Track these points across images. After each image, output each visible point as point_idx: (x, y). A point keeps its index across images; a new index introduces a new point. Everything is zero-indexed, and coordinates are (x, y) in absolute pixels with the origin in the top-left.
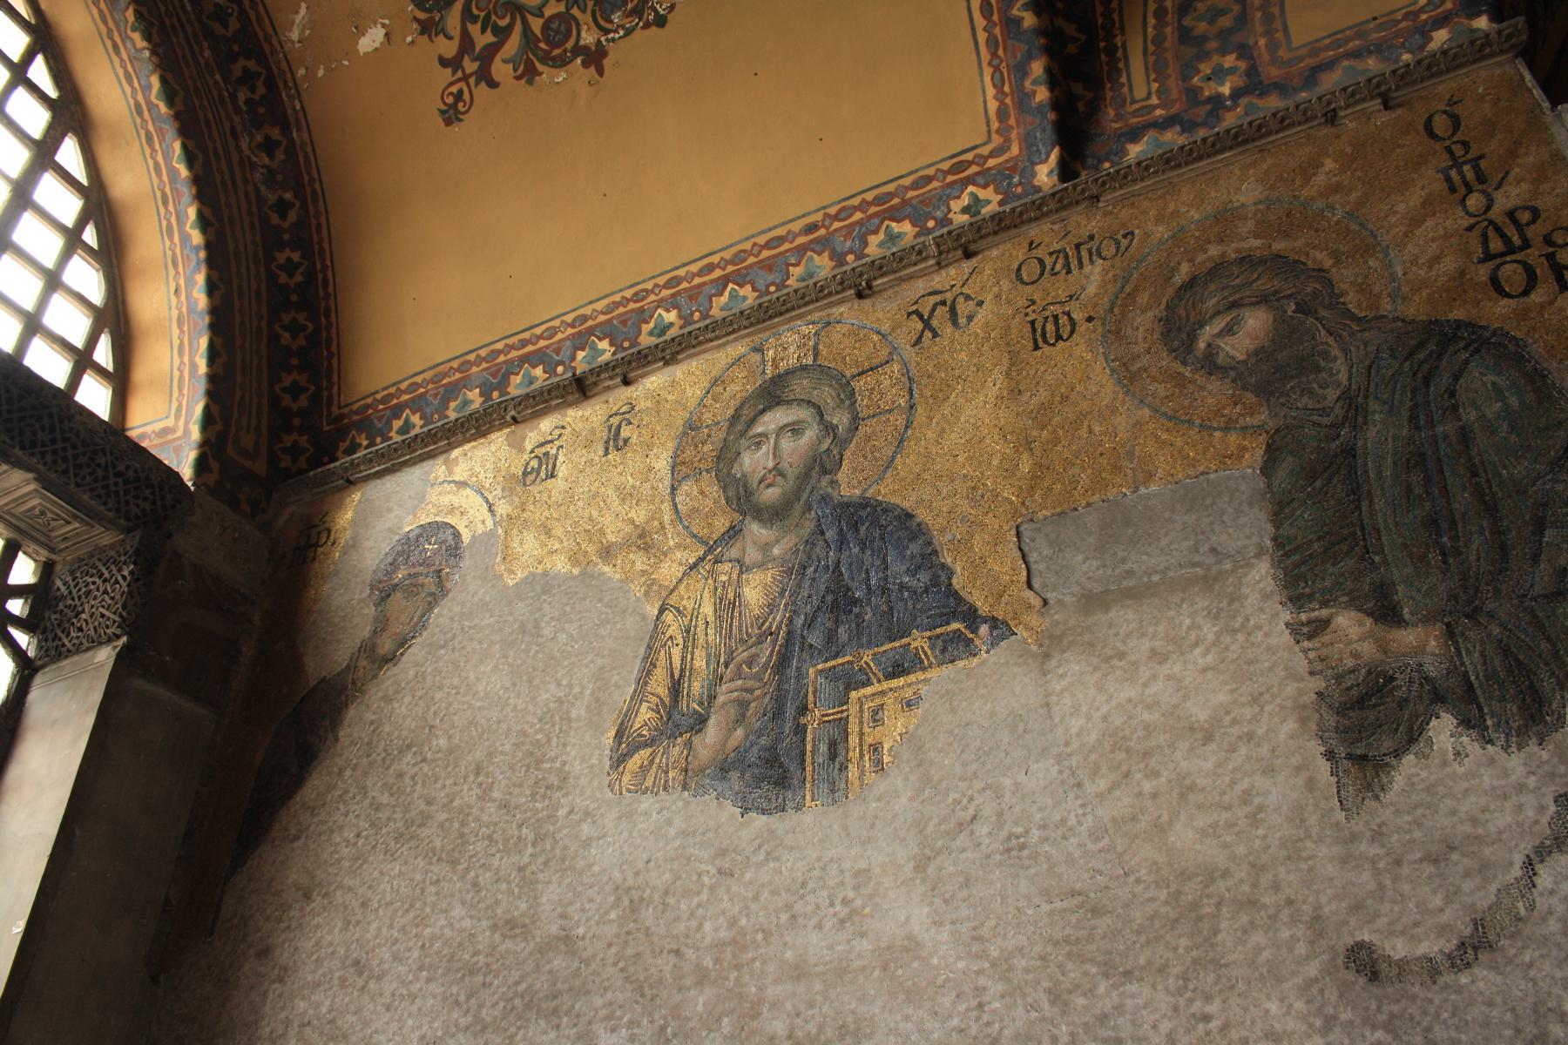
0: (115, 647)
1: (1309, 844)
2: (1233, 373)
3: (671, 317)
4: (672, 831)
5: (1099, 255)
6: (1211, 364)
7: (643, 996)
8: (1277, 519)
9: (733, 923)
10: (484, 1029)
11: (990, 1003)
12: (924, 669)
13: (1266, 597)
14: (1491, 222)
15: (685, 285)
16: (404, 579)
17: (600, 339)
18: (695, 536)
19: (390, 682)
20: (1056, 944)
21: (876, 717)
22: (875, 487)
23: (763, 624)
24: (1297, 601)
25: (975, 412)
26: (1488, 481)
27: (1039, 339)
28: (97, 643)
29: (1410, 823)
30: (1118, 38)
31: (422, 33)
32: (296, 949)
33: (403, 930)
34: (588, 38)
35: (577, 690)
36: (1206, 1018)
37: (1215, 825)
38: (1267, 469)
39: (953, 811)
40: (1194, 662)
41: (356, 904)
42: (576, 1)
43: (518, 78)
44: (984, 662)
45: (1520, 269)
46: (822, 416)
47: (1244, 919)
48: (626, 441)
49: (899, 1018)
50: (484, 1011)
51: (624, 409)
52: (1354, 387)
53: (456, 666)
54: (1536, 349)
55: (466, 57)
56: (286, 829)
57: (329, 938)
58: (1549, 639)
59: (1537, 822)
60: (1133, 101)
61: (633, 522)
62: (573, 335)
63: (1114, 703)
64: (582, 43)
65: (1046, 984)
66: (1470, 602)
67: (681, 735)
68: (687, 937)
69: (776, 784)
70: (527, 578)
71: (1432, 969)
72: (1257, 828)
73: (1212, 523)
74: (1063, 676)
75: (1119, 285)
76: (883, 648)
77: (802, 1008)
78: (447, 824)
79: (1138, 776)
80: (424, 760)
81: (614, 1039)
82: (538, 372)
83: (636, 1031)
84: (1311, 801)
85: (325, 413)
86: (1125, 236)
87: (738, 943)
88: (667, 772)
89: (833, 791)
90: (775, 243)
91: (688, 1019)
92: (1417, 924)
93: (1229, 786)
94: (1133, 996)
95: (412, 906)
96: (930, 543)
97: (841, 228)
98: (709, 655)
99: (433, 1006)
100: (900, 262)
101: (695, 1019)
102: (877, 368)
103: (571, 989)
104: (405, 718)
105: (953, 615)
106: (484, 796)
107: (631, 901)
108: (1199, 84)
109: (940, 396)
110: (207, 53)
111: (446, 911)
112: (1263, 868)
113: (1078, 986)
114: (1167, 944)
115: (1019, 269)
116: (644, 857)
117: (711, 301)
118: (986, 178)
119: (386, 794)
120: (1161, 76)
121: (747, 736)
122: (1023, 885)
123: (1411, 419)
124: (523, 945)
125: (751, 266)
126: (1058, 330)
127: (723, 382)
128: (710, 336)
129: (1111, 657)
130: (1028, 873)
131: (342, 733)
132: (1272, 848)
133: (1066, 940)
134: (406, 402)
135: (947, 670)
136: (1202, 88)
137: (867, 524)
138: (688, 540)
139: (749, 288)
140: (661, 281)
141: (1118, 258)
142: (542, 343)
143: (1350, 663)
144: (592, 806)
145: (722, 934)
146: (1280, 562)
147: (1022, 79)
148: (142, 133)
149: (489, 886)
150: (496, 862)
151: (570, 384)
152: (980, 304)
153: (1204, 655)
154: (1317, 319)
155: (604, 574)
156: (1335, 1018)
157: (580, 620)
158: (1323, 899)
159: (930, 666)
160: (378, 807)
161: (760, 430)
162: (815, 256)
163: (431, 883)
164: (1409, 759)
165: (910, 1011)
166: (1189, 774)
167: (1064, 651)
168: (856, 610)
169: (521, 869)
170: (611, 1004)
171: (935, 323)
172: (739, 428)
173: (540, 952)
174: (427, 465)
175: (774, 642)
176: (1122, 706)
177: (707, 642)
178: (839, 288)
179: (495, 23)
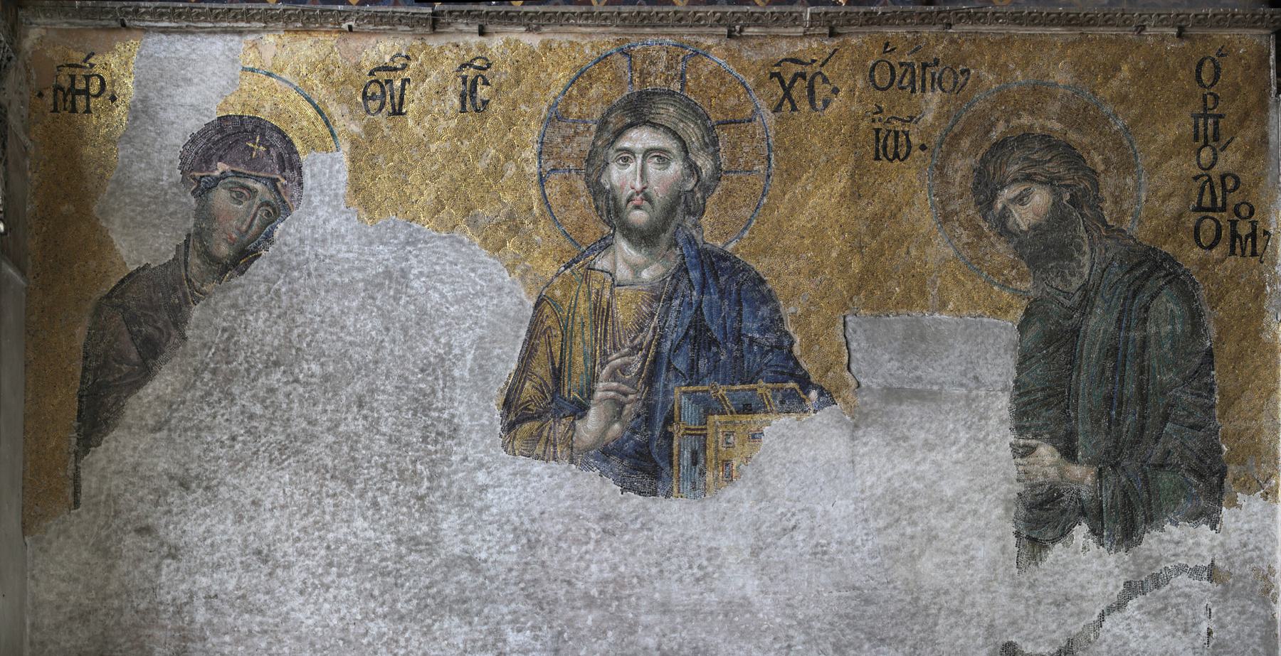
1: (995, 584)
4: (562, 494)
5: (940, 85)
7: (542, 609)
8: (1021, 366)
9: (614, 568)
10: (402, 618)
12: (766, 412)
13: (1002, 422)
14: (1210, 179)
16: (224, 175)
19: (238, 291)
20: (840, 617)
23: (635, 338)
24: (1020, 430)
25: (821, 201)
26: (1148, 380)
33: (304, 530)
35: (457, 351)
37: (945, 563)
38: (1022, 327)
39: (781, 520)
45: (1214, 227)
46: (687, 152)
47: (953, 620)
48: (485, 103)
49: (735, 647)
50: (399, 605)
51: (477, 63)
53: (315, 292)
54: (1203, 294)
56: (142, 418)
57: (222, 527)
58: (1148, 492)
59: (1112, 594)
63: (896, 471)
65: (832, 640)
66: (1115, 458)
67: (565, 416)
68: (577, 572)
74: (865, 444)
77: (667, 632)
80: (296, 381)
81: (520, 637)
83: (540, 634)
87: (619, 583)
88: (555, 446)
92: (1040, 637)
95: (309, 512)
96: (777, 311)
99: (348, 596)
101: (586, 629)
103: (478, 598)
104: (263, 333)
105: (792, 376)
107: (529, 541)
109: (791, 175)
111: (347, 521)
112: (968, 593)
113: (850, 644)
114: (907, 627)
115: (873, 69)
119: (259, 405)
121: (623, 432)
122: (823, 579)
123: (1119, 320)
124: (429, 559)
126: (896, 147)
127: (590, 76)
131: (188, 333)
133: (847, 616)
135: (784, 419)
137: (726, 276)
143: (1041, 479)
144: (486, 459)
145: (606, 575)
149: (388, 507)
152: (836, 91)
153: (958, 452)
158: (997, 616)
159: (772, 411)
161: (627, 145)
163: (328, 496)
164: (1059, 545)
165: (743, 644)
166: (935, 528)
167: (868, 426)
169: (420, 498)
170: (515, 612)
171: (794, 94)
172: (606, 135)
173: (446, 566)
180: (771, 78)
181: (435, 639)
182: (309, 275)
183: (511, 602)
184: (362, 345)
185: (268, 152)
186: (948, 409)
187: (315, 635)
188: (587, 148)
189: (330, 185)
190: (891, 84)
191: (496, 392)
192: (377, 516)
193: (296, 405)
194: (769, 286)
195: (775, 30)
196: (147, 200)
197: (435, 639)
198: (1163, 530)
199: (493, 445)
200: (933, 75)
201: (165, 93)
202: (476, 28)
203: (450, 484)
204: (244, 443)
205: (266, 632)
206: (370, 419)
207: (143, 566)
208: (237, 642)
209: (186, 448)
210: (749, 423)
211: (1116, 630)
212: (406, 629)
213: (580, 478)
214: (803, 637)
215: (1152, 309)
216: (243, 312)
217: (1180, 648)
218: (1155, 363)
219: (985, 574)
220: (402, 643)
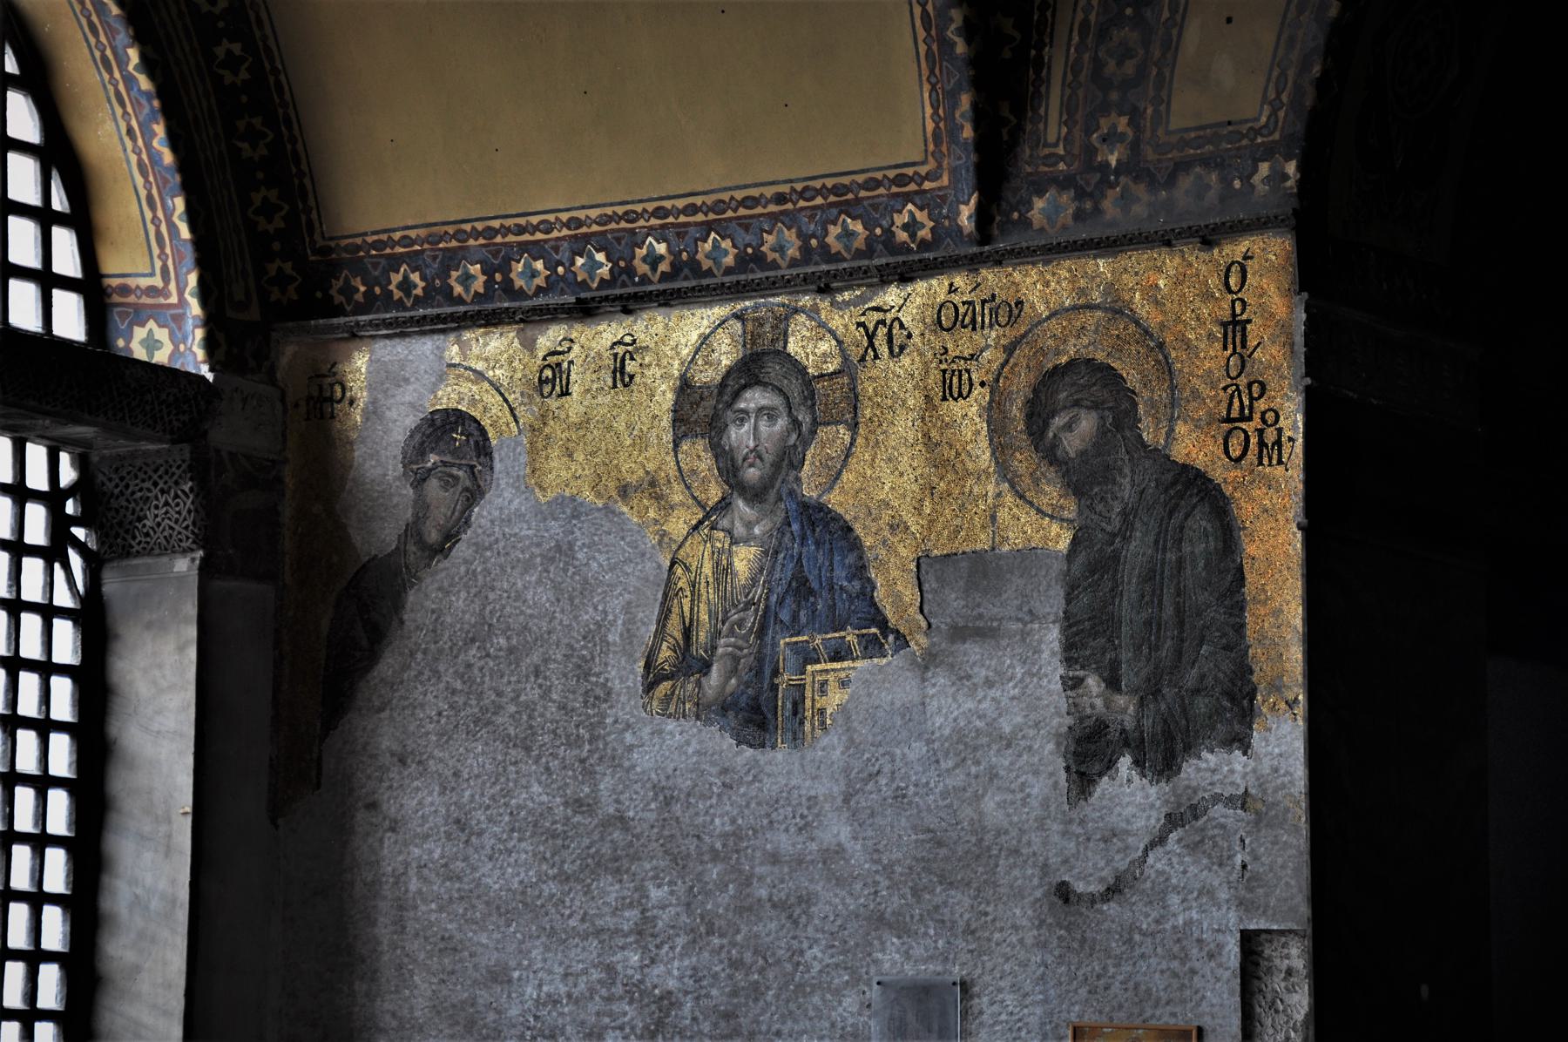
0: (193, 560)
1: (1048, 821)
3: (661, 248)
4: (690, 750)
7: (677, 864)
9: (733, 821)
10: (567, 879)
12: (853, 660)
13: (1053, 654)
14: (1237, 386)
15: (671, 220)
17: (598, 251)
18: (695, 498)
19: (443, 574)
20: (917, 860)
24: (1069, 661)
28: (170, 548)
30: (1047, 49)
32: (402, 805)
33: (493, 798)
35: (610, 617)
36: (986, 914)
37: (1005, 801)
41: (449, 773)
44: (889, 664)
47: (1012, 860)
50: (566, 866)
53: (502, 568)
56: (369, 700)
57: (430, 799)
60: (1046, 145)
62: (570, 237)
65: (910, 884)
66: (1156, 685)
71: (1092, 900)
74: (934, 685)
78: (517, 716)
79: (970, 762)
80: (488, 655)
82: (539, 265)
85: (307, 240)
87: (737, 835)
90: (749, 203)
91: (707, 883)
92: (1091, 875)
95: (497, 780)
96: (861, 558)
98: (710, 611)
103: (627, 855)
104: (464, 612)
106: (546, 694)
108: (1097, 145)
113: (926, 888)
115: (939, 311)
116: (672, 766)
117: (697, 246)
120: (1069, 122)
122: (903, 820)
123: (1156, 542)
125: (730, 219)
131: (405, 617)
133: (923, 858)
136: (1096, 150)
138: (690, 501)
139: (729, 241)
140: (650, 207)
142: (539, 236)
143: (1089, 711)
144: (632, 720)
153: (1014, 687)
156: (1044, 921)
158: (1050, 855)
160: (454, 692)
161: (742, 405)
164: (1106, 778)
167: (936, 667)
169: (582, 761)
171: (877, 343)
172: (726, 398)
175: (757, 611)
181: (593, 898)
182: (499, 553)
183: (652, 858)
184: (539, 617)
185: (468, 441)
187: (500, 898)
188: (710, 412)
189: (513, 467)
190: (955, 324)
191: (638, 655)
193: (487, 679)
196: (376, 494)
197: (593, 898)
198: (1200, 758)
199: (636, 707)
200: (991, 310)
201: (390, 393)
202: (619, 308)
203: (606, 744)
204: (448, 717)
205: (462, 898)
207: (370, 840)
208: (441, 909)
209: (404, 726)
210: (839, 670)
211: (1159, 866)
212: (570, 890)
213: (704, 734)
214: (887, 883)
215: (1186, 530)
216: (448, 593)
217: (1216, 883)
218: (1190, 583)
219: (1039, 812)
220: (568, 904)
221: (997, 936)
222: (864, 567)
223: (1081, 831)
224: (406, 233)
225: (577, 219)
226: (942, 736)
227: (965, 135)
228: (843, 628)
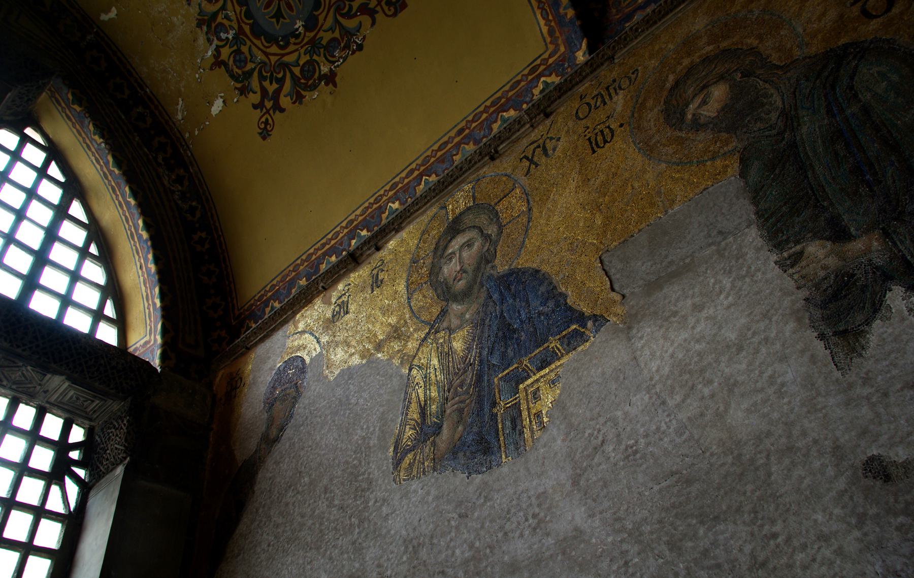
1: (820, 399)
2: (711, 126)
4: (430, 498)
6: (697, 125)
8: (755, 201)
9: (471, 546)
11: (631, 560)
12: (559, 359)
13: (758, 250)
17: (362, 230)
18: (423, 322)
19: (277, 453)
21: (536, 396)
22: (516, 261)
23: (466, 360)
24: (778, 246)
27: (594, 146)
28: (115, 465)
29: (887, 366)
31: (241, 95)
34: (325, 69)
35: (372, 429)
36: (775, 536)
37: (755, 404)
38: (743, 174)
39: (590, 441)
40: (722, 304)
42: (314, 52)
43: (294, 103)
46: (482, 232)
47: (787, 461)
52: (787, 107)
53: (309, 433)
55: (265, 100)
61: (390, 324)
62: (347, 232)
63: (676, 345)
64: (322, 73)
65: (665, 539)
68: (447, 561)
69: (485, 453)
70: (340, 373)
72: (784, 398)
73: (716, 216)
74: (641, 338)
75: (634, 101)
76: (534, 353)
78: (313, 526)
80: (298, 493)
84: (816, 370)
86: (633, 73)
88: (423, 463)
89: (517, 449)
90: (443, 147)
93: (759, 376)
94: (723, 533)
96: (551, 283)
97: (476, 126)
98: (439, 387)
100: (511, 130)
102: (508, 195)
105: (571, 322)
107: (414, 547)
110: (137, 138)
115: (577, 113)
117: (415, 190)
118: (549, 71)
125: (433, 163)
126: (604, 138)
127: (427, 231)
128: (416, 208)
129: (669, 317)
130: (642, 469)
131: (256, 489)
132: (797, 409)
133: (673, 506)
134: (271, 296)
140: (387, 188)
141: (631, 87)
142: (333, 242)
143: (822, 274)
146: (763, 226)
147: (558, 9)
148: (110, 188)
149: (338, 558)
150: (340, 542)
151: (348, 258)
152: (559, 139)
153: (727, 298)
154: (756, 77)
155: (379, 358)
156: (865, 514)
157: (369, 389)
159: (562, 356)
161: (450, 251)
162: (466, 146)
163: (308, 564)
164: (878, 322)
167: (639, 322)
168: (516, 336)
169: (354, 543)
174: (285, 328)
176: (681, 345)
177: (437, 381)
178: (480, 157)
179: (276, 77)
180: (521, 161)
186: (704, 269)
192: (332, 567)
194: (543, 272)
195: (514, 137)
196: (249, 426)
206: (329, 499)
214: (636, 548)
221: (800, 557)
222: (555, 288)
223: (870, 390)
224: (272, 283)
225: (351, 220)
226: (662, 376)
227: (569, 17)
228: (546, 340)
